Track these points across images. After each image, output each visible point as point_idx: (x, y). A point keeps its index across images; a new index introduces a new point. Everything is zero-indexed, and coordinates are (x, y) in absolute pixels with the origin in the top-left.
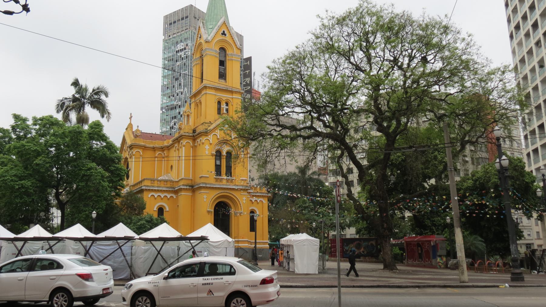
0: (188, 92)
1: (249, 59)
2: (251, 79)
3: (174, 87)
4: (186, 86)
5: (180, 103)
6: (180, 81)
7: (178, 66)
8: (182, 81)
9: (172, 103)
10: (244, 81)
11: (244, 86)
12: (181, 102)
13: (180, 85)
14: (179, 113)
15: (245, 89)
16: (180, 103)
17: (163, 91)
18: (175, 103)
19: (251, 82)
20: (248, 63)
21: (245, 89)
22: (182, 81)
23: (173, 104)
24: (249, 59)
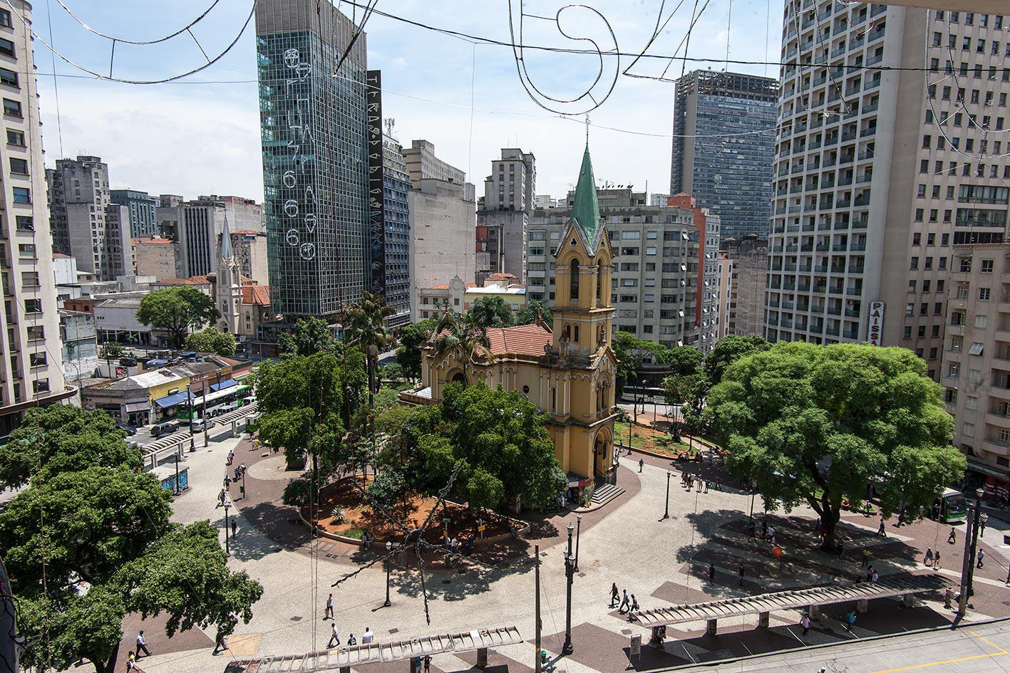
0: (312, 132)
1: (378, 73)
2: (380, 105)
3: (284, 119)
4: (308, 123)
5: (298, 146)
6: (296, 112)
7: (290, 86)
8: (300, 112)
9: (284, 144)
10: (369, 107)
11: (370, 114)
12: (301, 146)
13: (296, 117)
14: (298, 162)
15: (371, 119)
16: (298, 146)
17: (263, 119)
18: (289, 145)
19: (380, 109)
20: (376, 79)
21: (371, 119)
22: (300, 112)
23: (286, 147)
24: (378, 73)
